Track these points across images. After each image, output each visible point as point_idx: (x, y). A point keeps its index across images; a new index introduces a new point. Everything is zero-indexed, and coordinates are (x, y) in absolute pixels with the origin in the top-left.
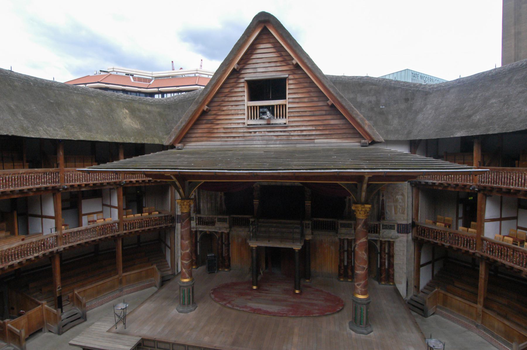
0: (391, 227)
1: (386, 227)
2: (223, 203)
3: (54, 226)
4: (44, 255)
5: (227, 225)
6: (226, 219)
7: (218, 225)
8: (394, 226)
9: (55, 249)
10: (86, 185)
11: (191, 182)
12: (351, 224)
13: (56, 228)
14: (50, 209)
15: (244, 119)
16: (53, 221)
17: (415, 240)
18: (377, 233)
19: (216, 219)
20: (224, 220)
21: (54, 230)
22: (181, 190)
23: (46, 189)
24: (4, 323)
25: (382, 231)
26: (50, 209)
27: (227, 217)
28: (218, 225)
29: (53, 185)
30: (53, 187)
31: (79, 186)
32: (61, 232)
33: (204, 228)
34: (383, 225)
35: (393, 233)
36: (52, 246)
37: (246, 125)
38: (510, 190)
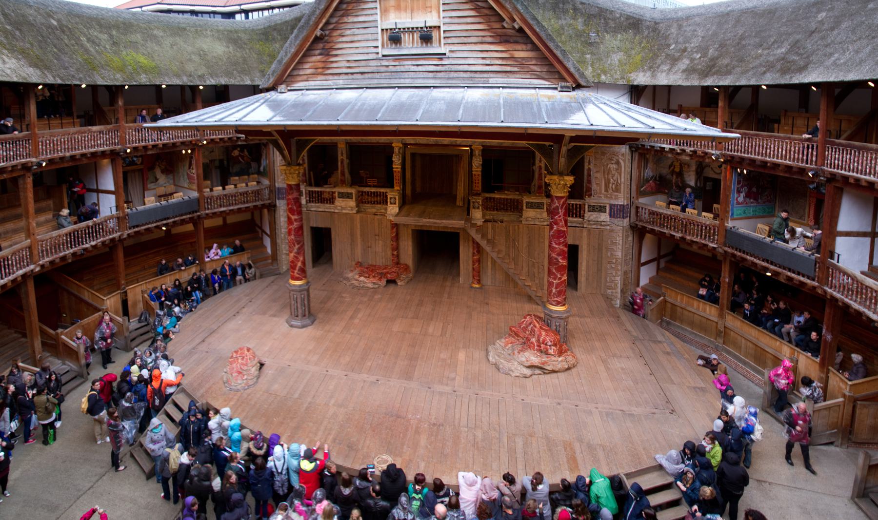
0: (601, 209)
1: (593, 209)
2: (346, 171)
3: (113, 204)
4: (103, 243)
5: (352, 203)
6: (351, 194)
7: (339, 202)
8: (605, 207)
9: (116, 235)
10: (154, 146)
11: (300, 140)
12: (542, 204)
13: (117, 207)
14: (108, 181)
15: (377, 47)
16: (112, 197)
17: (633, 228)
18: (580, 217)
19: (336, 194)
20: (348, 196)
21: (114, 209)
22: (286, 152)
23: (103, 152)
24: (57, 334)
25: (588, 215)
26: (108, 181)
27: (353, 191)
28: (339, 202)
29: (111, 147)
30: (112, 151)
31: (145, 147)
32: (123, 212)
33: (318, 207)
34: (589, 206)
35: (604, 217)
36: (113, 231)
37: (380, 56)
38: (766, 163)
